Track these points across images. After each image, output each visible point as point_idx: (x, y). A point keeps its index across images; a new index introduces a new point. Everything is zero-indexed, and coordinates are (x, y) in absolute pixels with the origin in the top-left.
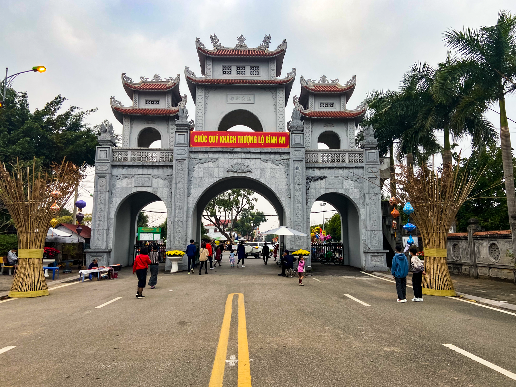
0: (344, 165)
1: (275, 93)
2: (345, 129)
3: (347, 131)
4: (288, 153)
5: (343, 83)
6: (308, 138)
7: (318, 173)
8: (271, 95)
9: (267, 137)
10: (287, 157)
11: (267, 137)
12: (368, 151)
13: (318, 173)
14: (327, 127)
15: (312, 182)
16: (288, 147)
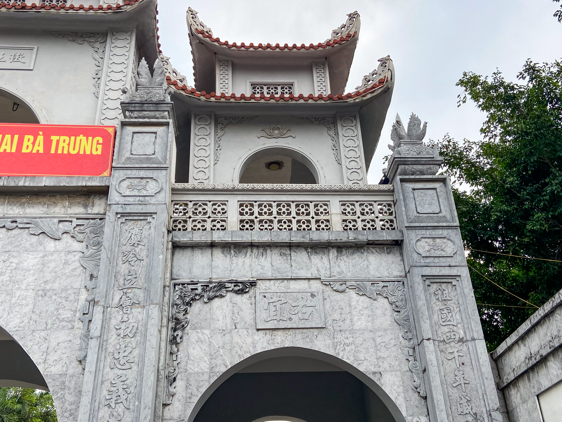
0: (325, 236)
1: (97, 45)
2: (330, 143)
3: (336, 148)
4: (103, 192)
5: (319, 34)
6: (202, 164)
7: (223, 267)
8: (91, 50)
9: (27, 137)
10: (98, 207)
11: (27, 137)
12: (410, 186)
13: (223, 267)
14: (271, 137)
15: (197, 307)
16: (106, 174)
